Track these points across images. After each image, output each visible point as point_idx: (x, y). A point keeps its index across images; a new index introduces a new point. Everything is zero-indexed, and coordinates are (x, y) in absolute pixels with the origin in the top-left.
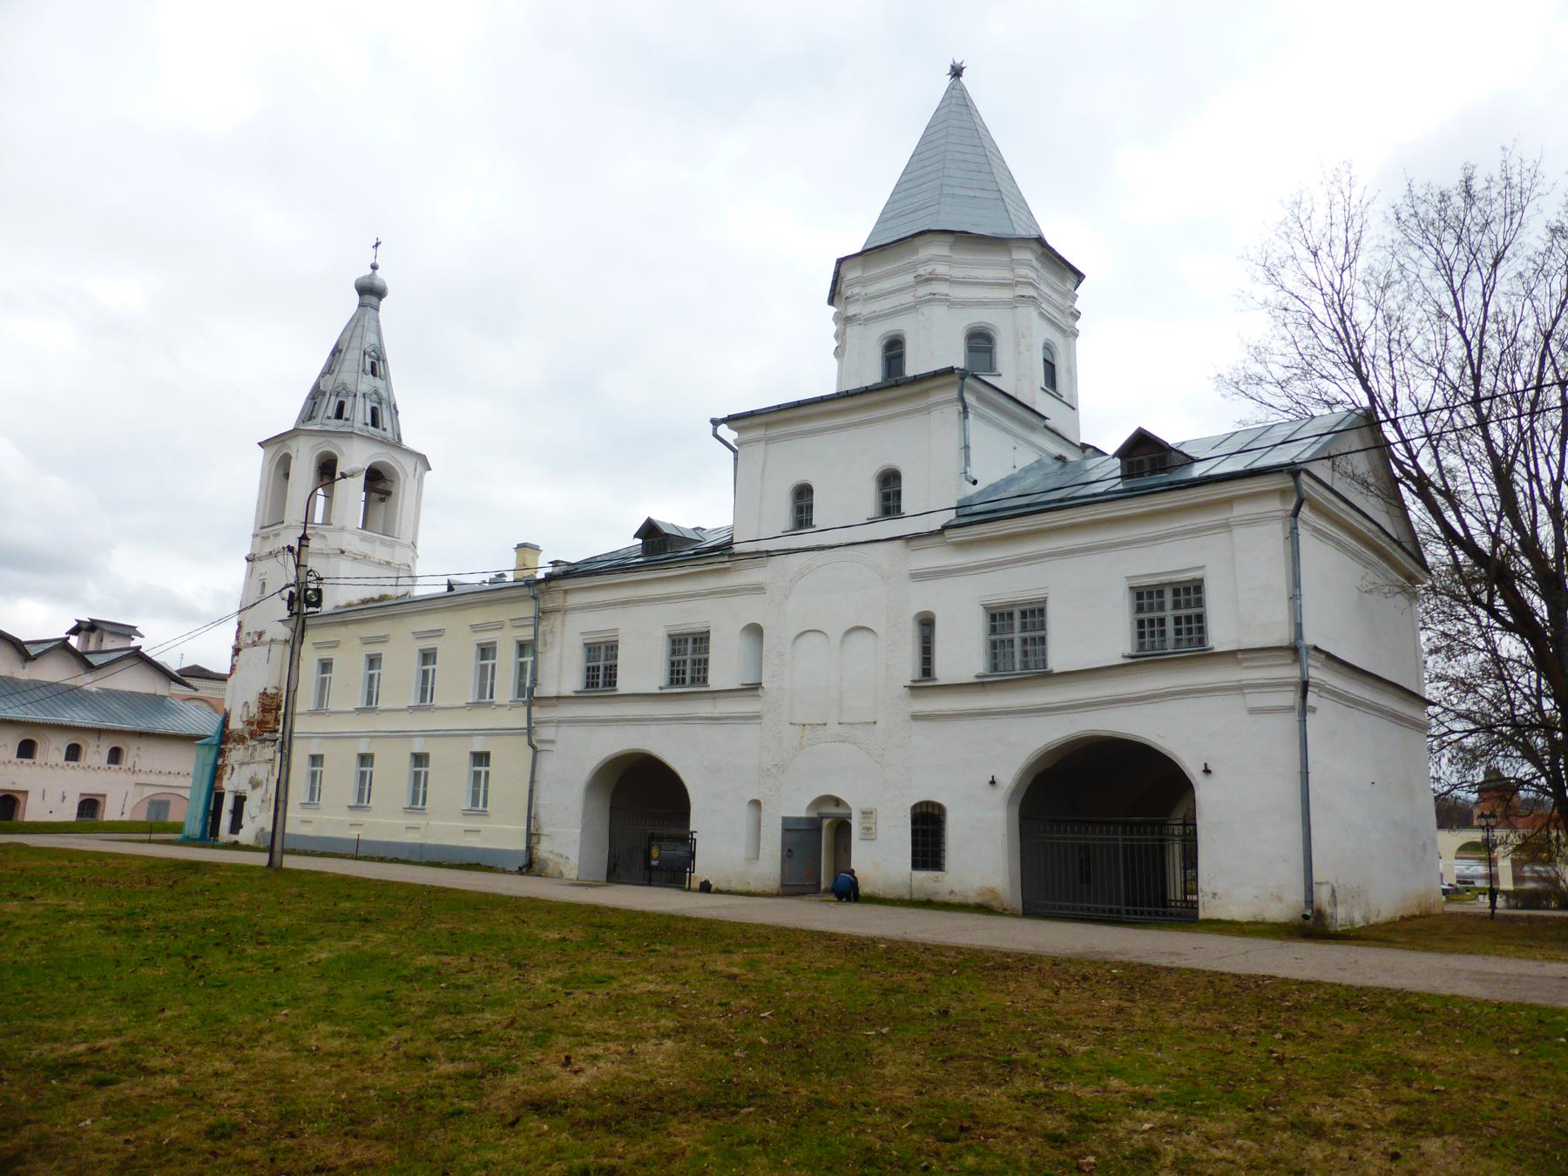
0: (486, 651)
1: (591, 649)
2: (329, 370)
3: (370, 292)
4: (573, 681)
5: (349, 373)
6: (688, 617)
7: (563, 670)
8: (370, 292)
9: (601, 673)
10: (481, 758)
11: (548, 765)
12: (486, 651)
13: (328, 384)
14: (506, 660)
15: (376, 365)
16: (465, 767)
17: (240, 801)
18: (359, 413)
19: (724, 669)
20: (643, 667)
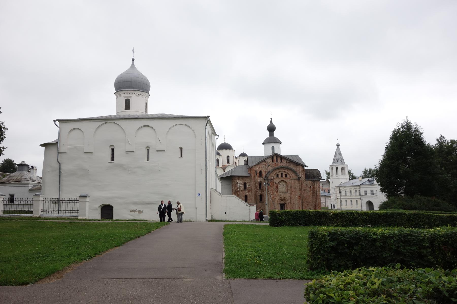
0: (356, 191)
1: (365, 191)
2: (335, 156)
3: (338, 146)
4: (364, 194)
5: (338, 157)
6: (372, 189)
7: (363, 193)
8: (338, 146)
9: (366, 194)
10: (357, 201)
11: (362, 202)
12: (356, 191)
13: (335, 158)
14: (358, 191)
15: (340, 155)
16: (356, 202)
17: (334, 205)
18: (339, 161)
19: (375, 195)
20: (369, 193)
